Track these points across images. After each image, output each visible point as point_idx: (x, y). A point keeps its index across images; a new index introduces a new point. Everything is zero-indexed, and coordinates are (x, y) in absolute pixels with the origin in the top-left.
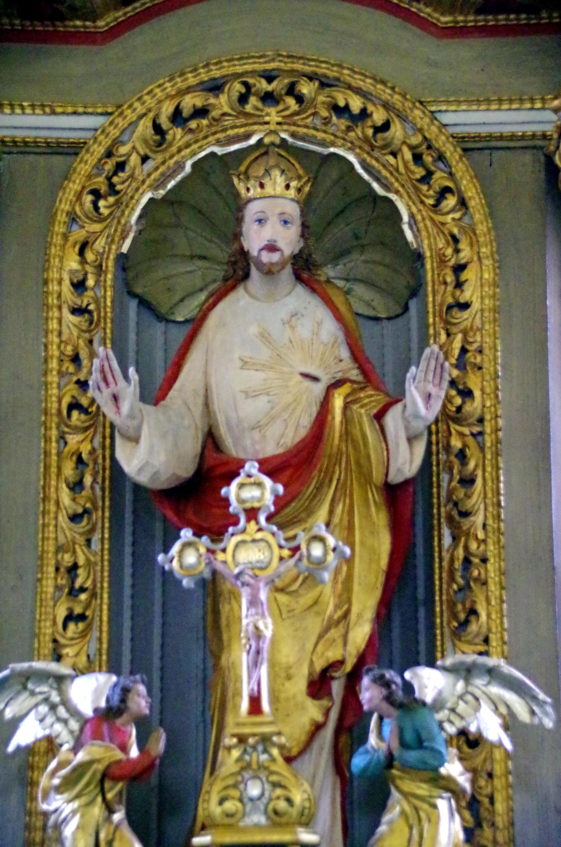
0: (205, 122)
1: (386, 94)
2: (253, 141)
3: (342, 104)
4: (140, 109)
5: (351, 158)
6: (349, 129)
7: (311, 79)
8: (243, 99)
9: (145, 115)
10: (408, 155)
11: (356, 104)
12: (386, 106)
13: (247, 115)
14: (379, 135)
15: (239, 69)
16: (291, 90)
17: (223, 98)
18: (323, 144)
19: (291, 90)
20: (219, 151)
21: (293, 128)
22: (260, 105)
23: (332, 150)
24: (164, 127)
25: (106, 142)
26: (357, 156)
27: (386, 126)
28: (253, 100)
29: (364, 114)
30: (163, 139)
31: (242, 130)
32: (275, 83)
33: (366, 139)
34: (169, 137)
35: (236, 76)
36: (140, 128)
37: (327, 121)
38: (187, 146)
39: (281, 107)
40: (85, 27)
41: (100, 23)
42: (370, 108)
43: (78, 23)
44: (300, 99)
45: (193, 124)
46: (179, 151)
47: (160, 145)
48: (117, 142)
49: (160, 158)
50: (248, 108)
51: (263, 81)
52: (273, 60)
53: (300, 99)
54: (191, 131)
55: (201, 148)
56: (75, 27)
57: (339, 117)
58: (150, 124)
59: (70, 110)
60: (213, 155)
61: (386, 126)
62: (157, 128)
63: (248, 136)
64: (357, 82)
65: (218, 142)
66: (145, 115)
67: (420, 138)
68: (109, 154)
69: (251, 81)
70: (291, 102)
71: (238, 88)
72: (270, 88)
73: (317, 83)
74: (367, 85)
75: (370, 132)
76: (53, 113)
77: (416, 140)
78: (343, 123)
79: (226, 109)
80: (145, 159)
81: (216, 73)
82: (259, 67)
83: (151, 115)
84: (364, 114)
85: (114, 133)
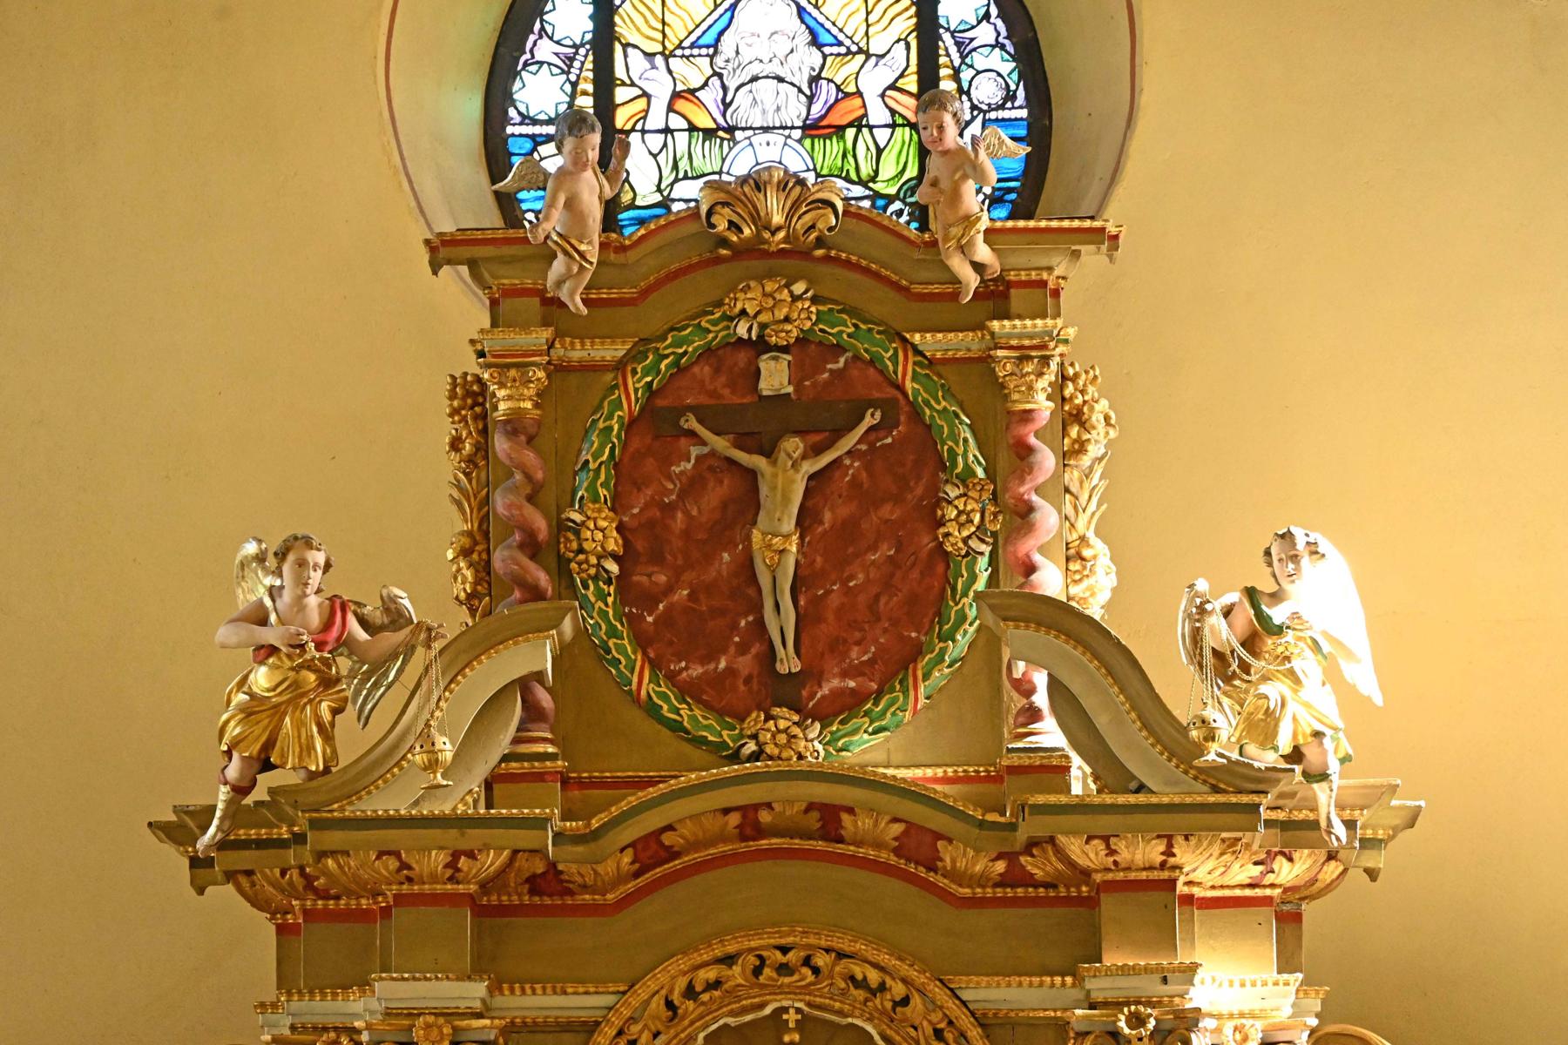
0: (717, 993)
1: (905, 969)
2: (768, 1011)
3: (859, 977)
4: (653, 987)
5: (869, 1028)
6: (866, 1000)
7: (827, 951)
8: (757, 971)
9: (657, 992)
10: (929, 1031)
11: (874, 977)
12: (904, 981)
13: (763, 986)
14: (899, 1009)
15: (753, 944)
16: (807, 961)
17: (737, 969)
18: (840, 1013)
19: (807, 961)
20: (731, 1021)
21: (807, 998)
22: (774, 975)
23: (850, 1020)
24: (676, 1002)
25: (618, 1022)
26: (875, 1027)
27: (905, 1001)
28: (767, 971)
29: (882, 987)
30: (675, 1014)
31: (757, 1000)
32: (791, 955)
33: (883, 1012)
34: (680, 1011)
35: (751, 950)
36: (653, 1005)
37: (844, 993)
38: (701, 1017)
39: (796, 977)
40: (594, 900)
41: (609, 896)
42: (889, 982)
43: (587, 897)
44: (816, 971)
45: (705, 997)
46: (692, 1023)
47: (671, 1020)
48: (632, 1020)
49: (672, 1032)
50: (762, 979)
51: (778, 954)
52: (789, 935)
53: (816, 971)
54: (703, 1003)
55: (715, 1020)
56: (584, 900)
57: (856, 987)
58: (662, 1002)
59: (581, 990)
60: (726, 1025)
61: (905, 1001)
62: (670, 1005)
63: (762, 1006)
64: (871, 954)
65: (732, 1014)
66: (657, 992)
67: (940, 1015)
68: (620, 1033)
69: (764, 953)
70: (806, 971)
71: (752, 960)
72: (784, 960)
73: (833, 955)
74: (884, 958)
75: (889, 1005)
76: (565, 993)
77: (936, 1017)
78: (860, 994)
79: (741, 981)
80: (656, 1035)
81: (731, 948)
82: (772, 941)
83: (664, 992)
84: (882, 987)
85: (626, 1013)
